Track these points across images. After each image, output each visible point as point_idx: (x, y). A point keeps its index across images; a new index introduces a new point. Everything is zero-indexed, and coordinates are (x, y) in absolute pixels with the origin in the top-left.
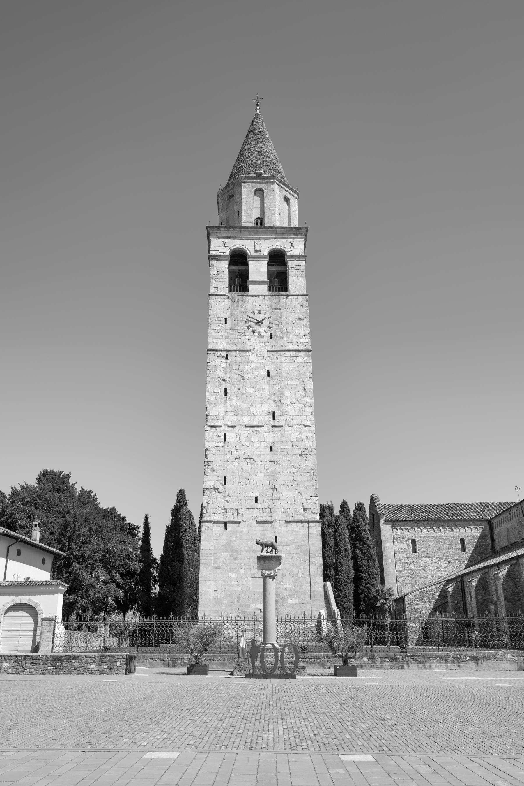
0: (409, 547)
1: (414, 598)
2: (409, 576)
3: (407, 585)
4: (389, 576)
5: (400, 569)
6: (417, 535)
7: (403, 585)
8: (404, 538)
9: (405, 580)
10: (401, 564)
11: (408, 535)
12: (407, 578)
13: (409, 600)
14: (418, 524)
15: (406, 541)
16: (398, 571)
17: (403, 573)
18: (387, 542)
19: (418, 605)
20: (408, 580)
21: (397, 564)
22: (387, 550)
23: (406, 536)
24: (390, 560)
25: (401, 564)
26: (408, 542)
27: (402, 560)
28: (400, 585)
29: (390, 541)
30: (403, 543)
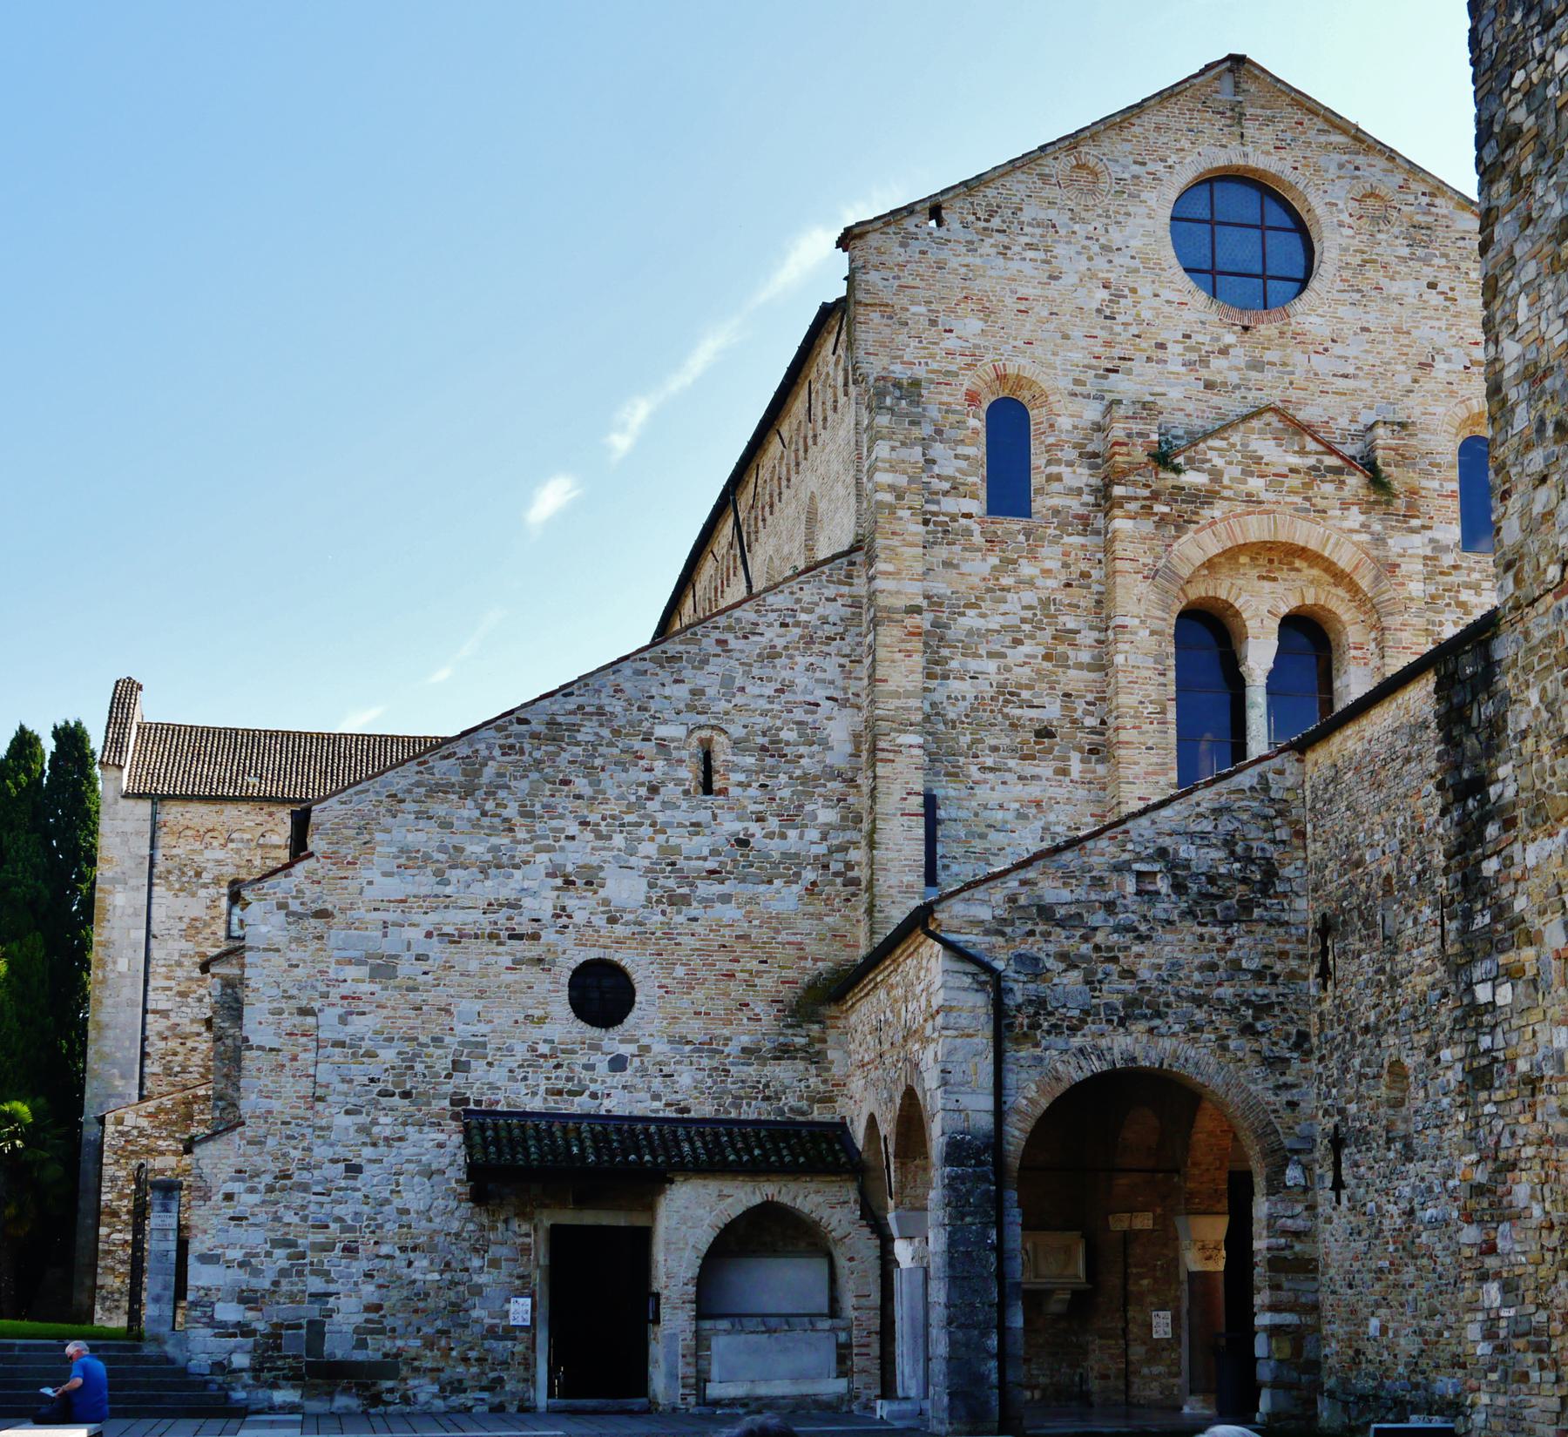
0: (214, 913)
1: (144, 1123)
2: (199, 1034)
3: (183, 1071)
4: (110, 1033)
5: (162, 1006)
6: (257, 862)
7: (168, 1071)
8: (198, 875)
9: (180, 1049)
10: (172, 983)
11: (217, 861)
12: (190, 1044)
13: (122, 1134)
14: (271, 814)
15: (205, 886)
16: (155, 1012)
17: (177, 1020)
18: (119, 887)
19: (162, 1153)
20: (194, 1049)
21: (152, 983)
22: (115, 922)
23: (210, 865)
24: (122, 965)
25: (172, 983)
26: (212, 891)
27: (179, 964)
28: (156, 1069)
29: (132, 882)
30: (193, 895)
